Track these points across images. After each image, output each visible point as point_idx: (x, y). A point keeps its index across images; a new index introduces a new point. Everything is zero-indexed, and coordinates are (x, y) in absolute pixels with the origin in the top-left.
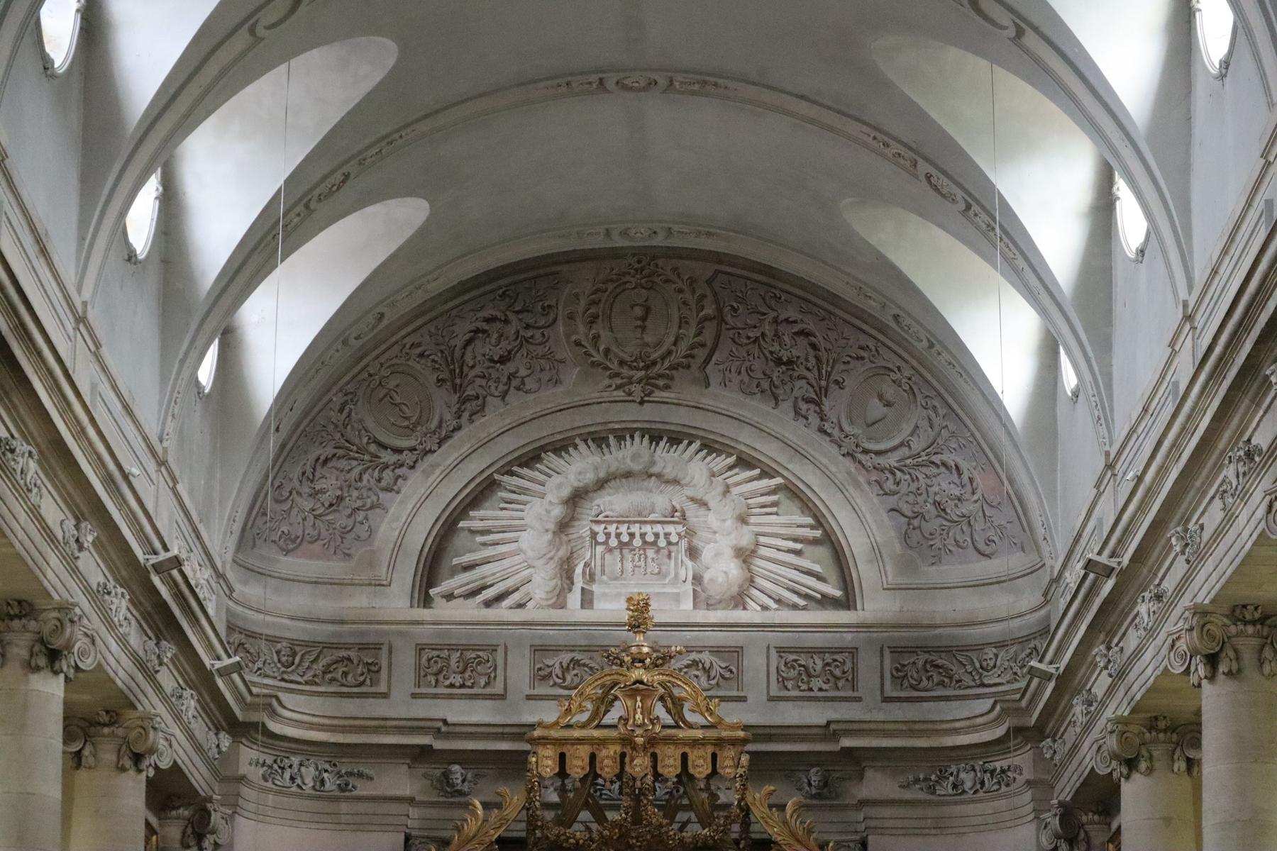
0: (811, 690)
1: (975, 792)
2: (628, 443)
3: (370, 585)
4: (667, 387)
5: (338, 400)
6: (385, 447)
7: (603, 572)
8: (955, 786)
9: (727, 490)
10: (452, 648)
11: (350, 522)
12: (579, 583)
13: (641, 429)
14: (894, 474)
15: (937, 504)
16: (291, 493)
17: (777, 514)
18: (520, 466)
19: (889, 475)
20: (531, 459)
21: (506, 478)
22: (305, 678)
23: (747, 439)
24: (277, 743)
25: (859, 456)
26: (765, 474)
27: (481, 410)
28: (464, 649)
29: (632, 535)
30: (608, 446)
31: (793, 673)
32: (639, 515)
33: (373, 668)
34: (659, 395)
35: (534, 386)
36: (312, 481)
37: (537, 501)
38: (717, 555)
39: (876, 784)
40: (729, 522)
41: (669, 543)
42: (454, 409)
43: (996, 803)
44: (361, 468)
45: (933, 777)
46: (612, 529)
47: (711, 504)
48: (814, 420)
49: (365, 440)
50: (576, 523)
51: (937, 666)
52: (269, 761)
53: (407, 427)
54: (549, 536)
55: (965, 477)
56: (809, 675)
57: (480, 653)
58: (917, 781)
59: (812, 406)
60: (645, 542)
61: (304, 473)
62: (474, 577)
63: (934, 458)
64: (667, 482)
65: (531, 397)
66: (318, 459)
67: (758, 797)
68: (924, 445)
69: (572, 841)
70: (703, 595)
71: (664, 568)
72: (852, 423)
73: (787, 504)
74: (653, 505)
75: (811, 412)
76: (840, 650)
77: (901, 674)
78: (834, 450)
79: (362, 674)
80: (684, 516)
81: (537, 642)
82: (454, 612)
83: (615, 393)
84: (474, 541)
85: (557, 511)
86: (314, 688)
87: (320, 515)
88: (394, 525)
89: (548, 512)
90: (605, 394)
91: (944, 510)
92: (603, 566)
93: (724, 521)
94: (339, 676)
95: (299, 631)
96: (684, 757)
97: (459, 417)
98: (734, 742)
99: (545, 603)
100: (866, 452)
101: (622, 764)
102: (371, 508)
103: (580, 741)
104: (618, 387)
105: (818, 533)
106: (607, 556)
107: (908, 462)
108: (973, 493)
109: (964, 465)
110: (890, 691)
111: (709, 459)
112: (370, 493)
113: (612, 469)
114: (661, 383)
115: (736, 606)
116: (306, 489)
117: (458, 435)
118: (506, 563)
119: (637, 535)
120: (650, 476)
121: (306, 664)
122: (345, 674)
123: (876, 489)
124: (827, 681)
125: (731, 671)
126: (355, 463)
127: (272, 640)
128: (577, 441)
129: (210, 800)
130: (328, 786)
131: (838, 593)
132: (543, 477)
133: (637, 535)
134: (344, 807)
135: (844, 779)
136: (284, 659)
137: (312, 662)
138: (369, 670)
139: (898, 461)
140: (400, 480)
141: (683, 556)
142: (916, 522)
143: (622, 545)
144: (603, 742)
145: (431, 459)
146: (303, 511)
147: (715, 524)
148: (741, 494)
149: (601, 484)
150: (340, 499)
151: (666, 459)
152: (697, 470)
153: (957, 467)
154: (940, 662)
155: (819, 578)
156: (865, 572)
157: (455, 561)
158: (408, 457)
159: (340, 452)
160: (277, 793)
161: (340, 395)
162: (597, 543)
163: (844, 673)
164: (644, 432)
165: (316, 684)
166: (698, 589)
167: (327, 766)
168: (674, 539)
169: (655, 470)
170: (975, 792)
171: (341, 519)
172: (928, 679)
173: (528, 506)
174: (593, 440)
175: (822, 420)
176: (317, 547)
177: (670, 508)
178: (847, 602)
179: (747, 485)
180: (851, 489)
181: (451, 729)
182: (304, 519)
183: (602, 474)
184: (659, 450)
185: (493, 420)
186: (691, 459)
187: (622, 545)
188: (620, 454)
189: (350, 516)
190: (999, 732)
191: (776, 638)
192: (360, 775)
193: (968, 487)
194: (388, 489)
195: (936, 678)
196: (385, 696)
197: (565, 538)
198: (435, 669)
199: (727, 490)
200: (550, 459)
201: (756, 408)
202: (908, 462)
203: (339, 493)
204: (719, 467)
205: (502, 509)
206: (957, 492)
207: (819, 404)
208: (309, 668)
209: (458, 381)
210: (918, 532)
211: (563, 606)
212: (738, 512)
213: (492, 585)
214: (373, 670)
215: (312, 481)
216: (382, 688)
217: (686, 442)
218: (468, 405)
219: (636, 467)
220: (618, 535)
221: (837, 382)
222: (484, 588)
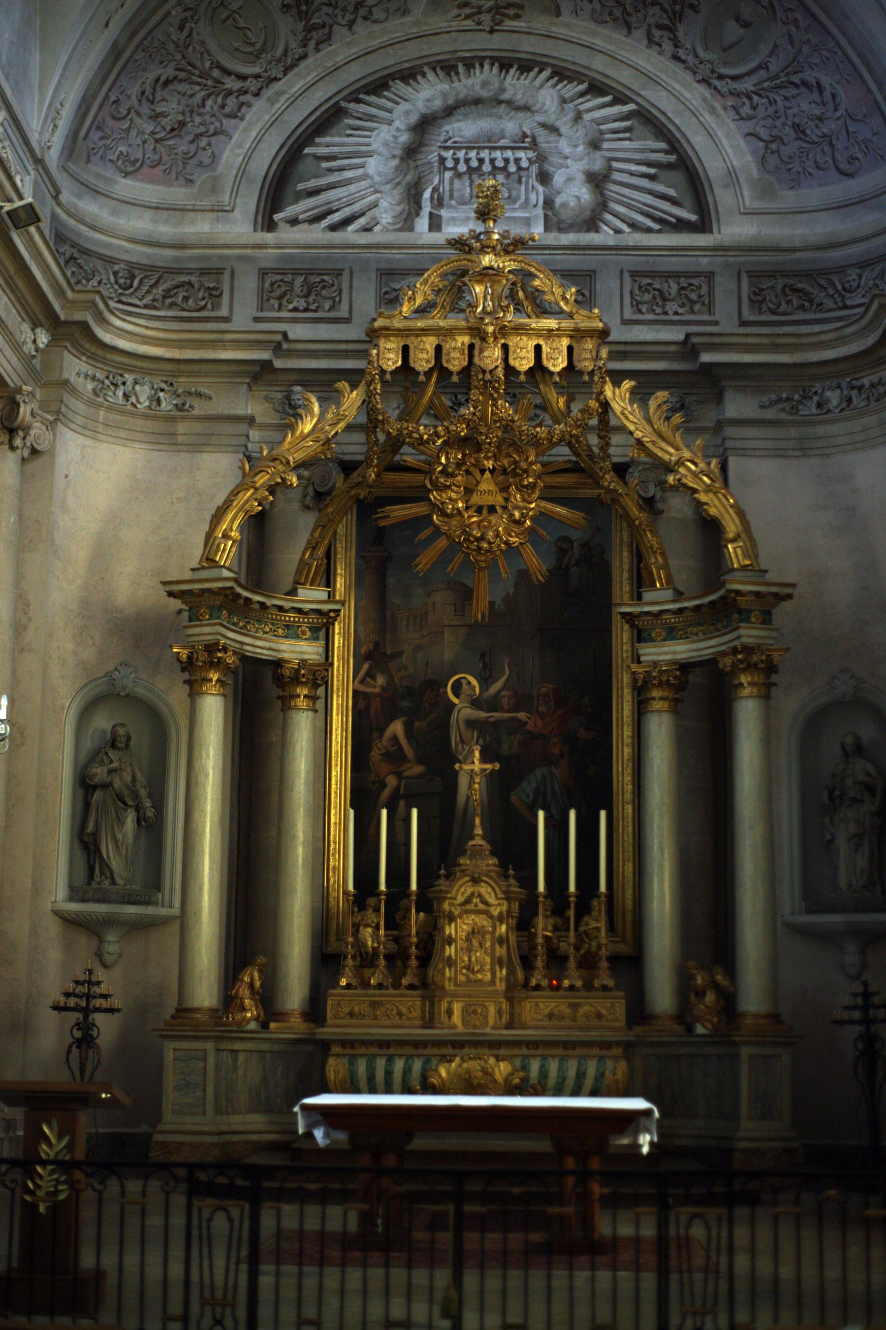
0: (666, 313)
1: (841, 411)
2: (478, 71)
3: (212, 210)
4: (517, 17)
5: (177, 14)
6: (229, 73)
7: (451, 197)
8: (819, 405)
9: (578, 117)
10: (296, 272)
11: (193, 148)
12: (427, 208)
13: (491, 57)
14: (750, 98)
15: (796, 126)
16: (129, 111)
17: (630, 139)
18: (368, 93)
19: (746, 100)
20: (378, 86)
21: (352, 106)
22: (144, 301)
23: (598, 64)
24: (110, 356)
25: (715, 82)
26: (620, 100)
27: (327, 39)
28: (309, 272)
29: (481, 161)
30: (457, 74)
31: (647, 297)
32: (489, 141)
33: (214, 293)
34: (509, 24)
35: (382, 16)
36: (152, 102)
37: (385, 128)
38: (570, 179)
39: (737, 405)
40: (581, 148)
41: (520, 168)
42: (300, 37)
43: (865, 420)
44: (203, 93)
45: (796, 397)
46: (461, 154)
47: (563, 130)
48: (668, 46)
49: (208, 64)
50: (424, 149)
51: (797, 290)
52: (100, 375)
53: (251, 53)
54: (395, 162)
55: (827, 95)
56: (665, 300)
57: (326, 278)
58: (780, 400)
59: (666, 34)
60: (495, 168)
61: (143, 93)
62: (319, 202)
63: (795, 79)
64: (519, 109)
65: (377, 28)
66: (158, 80)
67: (618, 397)
68: (783, 65)
69: (415, 435)
70: (555, 220)
71: (514, 193)
72: (707, 48)
73: (639, 129)
74: (503, 130)
75: (665, 39)
76: (696, 275)
77: (758, 298)
78: (688, 76)
79: (203, 299)
80: (534, 143)
81: (383, 266)
82: (296, 237)
83: (465, 23)
84: (319, 167)
85: (404, 138)
86: (153, 312)
87: (161, 139)
88: (237, 151)
89: (395, 137)
90: (454, 23)
91: (803, 132)
92: (451, 191)
93: (576, 146)
94: (179, 300)
95: (139, 254)
96: (538, 349)
97: (305, 46)
98: (590, 333)
99: (391, 228)
100: (721, 77)
101: (471, 356)
102: (214, 135)
103: (425, 332)
104: (467, 17)
105: (672, 158)
106: (456, 182)
107: (766, 84)
108: (836, 110)
109: (826, 81)
110: (747, 315)
111: (560, 86)
112: (213, 119)
113: (461, 96)
114: (511, 12)
115: (588, 230)
116: (145, 110)
117: (304, 64)
118: (352, 188)
119: (487, 160)
120: (500, 102)
121: (145, 288)
122: (186, 299)
123: (732, 113)
124: (683, 306)
125: (583, 295)
126: (197, 88)
127: (110, 261)
128: (426, 69)
129: (19, 391)
130: (164, 404)
131: (693, 217)
132: (390, 105)
133: (487, 160)
134: (182, 428)
135: (701, 403)
136: (121, 281)
137: (152, 286)
138: (210, 295)
139: (755, 85)
140: (244, 109)
141: (533, 181)
142: (774, 146)
143: (471, 170)
144: (450, 333)
145: (276, 86)
146: (143, 133)
147: (567, 150)
148: (593, 121)
149: (449, 111)
150: (182, 124)
151: (515, 85)
152: (548, 97)
153: (818, 84)
154: (799, 286)
155: (674, 202)
156: (722, 197)
157: (300, 186)
158: (252, 85)
159: (182, 75)
160: (110, 409)
161: (180, 9)
162: (446, 169)
163: (700, 297)
164: (493, 60)
165: (155, 308)
166: (550, 213)
167: (163, 386)
168: (524, 164)
169: (506, 96)
170: (841, 411)
171: (183, 146)
172: (788, 302)
173: (375, 133)
174: (442, 68)
175: (676, 46)
176: (158, 171)
177: (520, 134)
178: (703, 226)
179: (598, 110)
180: (707, 115)
181: (293, 346)
182: (144, 142)
183: (451, 101)
184: (509, 79)
185: (339, 50)
186: (541, 86)
187: (471, 170)
188: (470, 81)
189: (192, 142)
190: (870, 340)
191: (631, 261)
192: (199, 395)
193: (831, 106)
194: (232, 116)
195: (796, 303)
196: (227, 320)
197: (412, 164)
198: (278, 293)
199: (578, 117)
200: (398, 86)
201: (606, 38)
202: (766, 84)
203: (181, 118)
204: (571, 93)
205: (349, 135)
206: (817, 111)
207: (672, 30)
208: (148, 292)
209: (304, 8)
210: (776, 155)
211: (411, 229)
212: (589, 138)
213: (337, 210)
214: (214, 295)
215: (152, 102)
216: (224, 312)
217: (536, 70)
218: (314, 34)
219: (485, 94)
220: (467, 161)
221: (692, 6)
222: (330, 212)
